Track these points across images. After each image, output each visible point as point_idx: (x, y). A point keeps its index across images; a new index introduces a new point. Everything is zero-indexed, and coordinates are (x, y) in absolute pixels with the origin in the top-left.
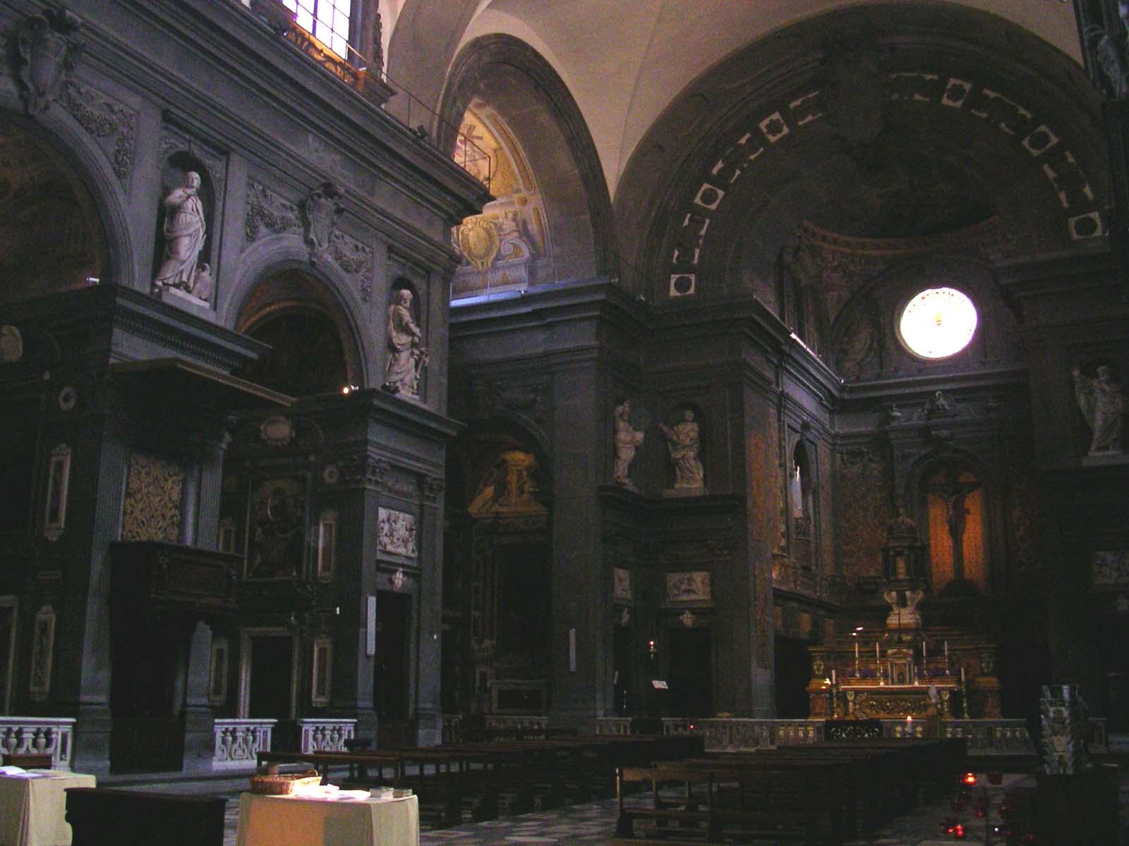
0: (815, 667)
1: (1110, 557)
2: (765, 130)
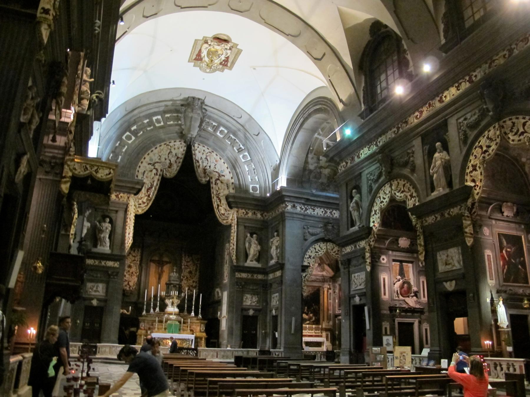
0: (140, 325)
1: (249, 296)
2: (155, 121)
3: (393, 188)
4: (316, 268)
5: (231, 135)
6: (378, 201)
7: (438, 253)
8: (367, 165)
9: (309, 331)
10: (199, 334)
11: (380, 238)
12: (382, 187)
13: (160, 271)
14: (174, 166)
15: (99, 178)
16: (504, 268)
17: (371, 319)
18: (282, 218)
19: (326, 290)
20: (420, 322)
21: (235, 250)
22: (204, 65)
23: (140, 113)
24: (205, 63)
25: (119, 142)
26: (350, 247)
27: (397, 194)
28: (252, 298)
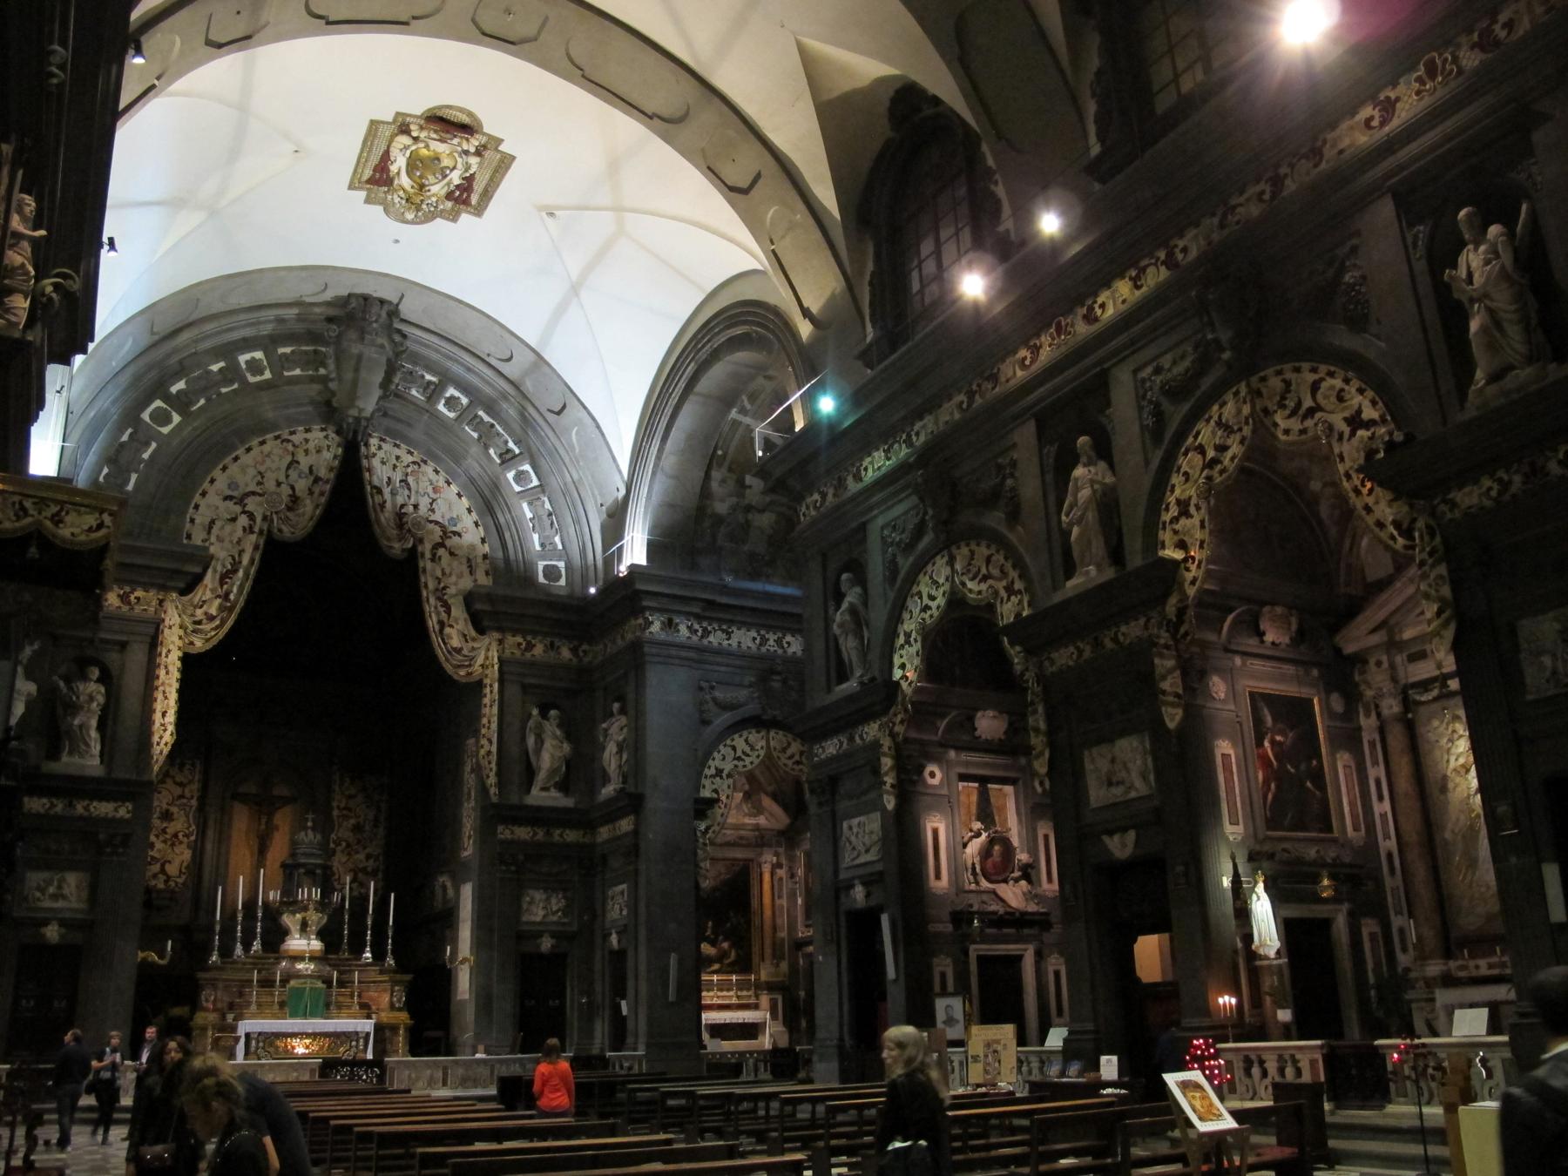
0: (203, 998)
1: (539, 895)
2: (244, 366)
3: (958, 567)
4: (739, 807)
5: (481, 413)
6: (914, 606)
7: (1086, 753)
8: (884, 501)
9: (719, 994)
10: (386, 1017)
11: (922, 712)
12: (927, 563)
13: (263, 827)
14: (305, 506)
15: (64, 540)
16: (1269, 789)
17: (901, 948)
18: (636, 656)
19: (766, 869)
20: (1039, 956)
21: (494, 758)
22: (397, 200)
23: (196, 341)
24: (401, 193)
25: (130, 431)
26: (835, 741)
27: (970, 585)
28: (548, 899)
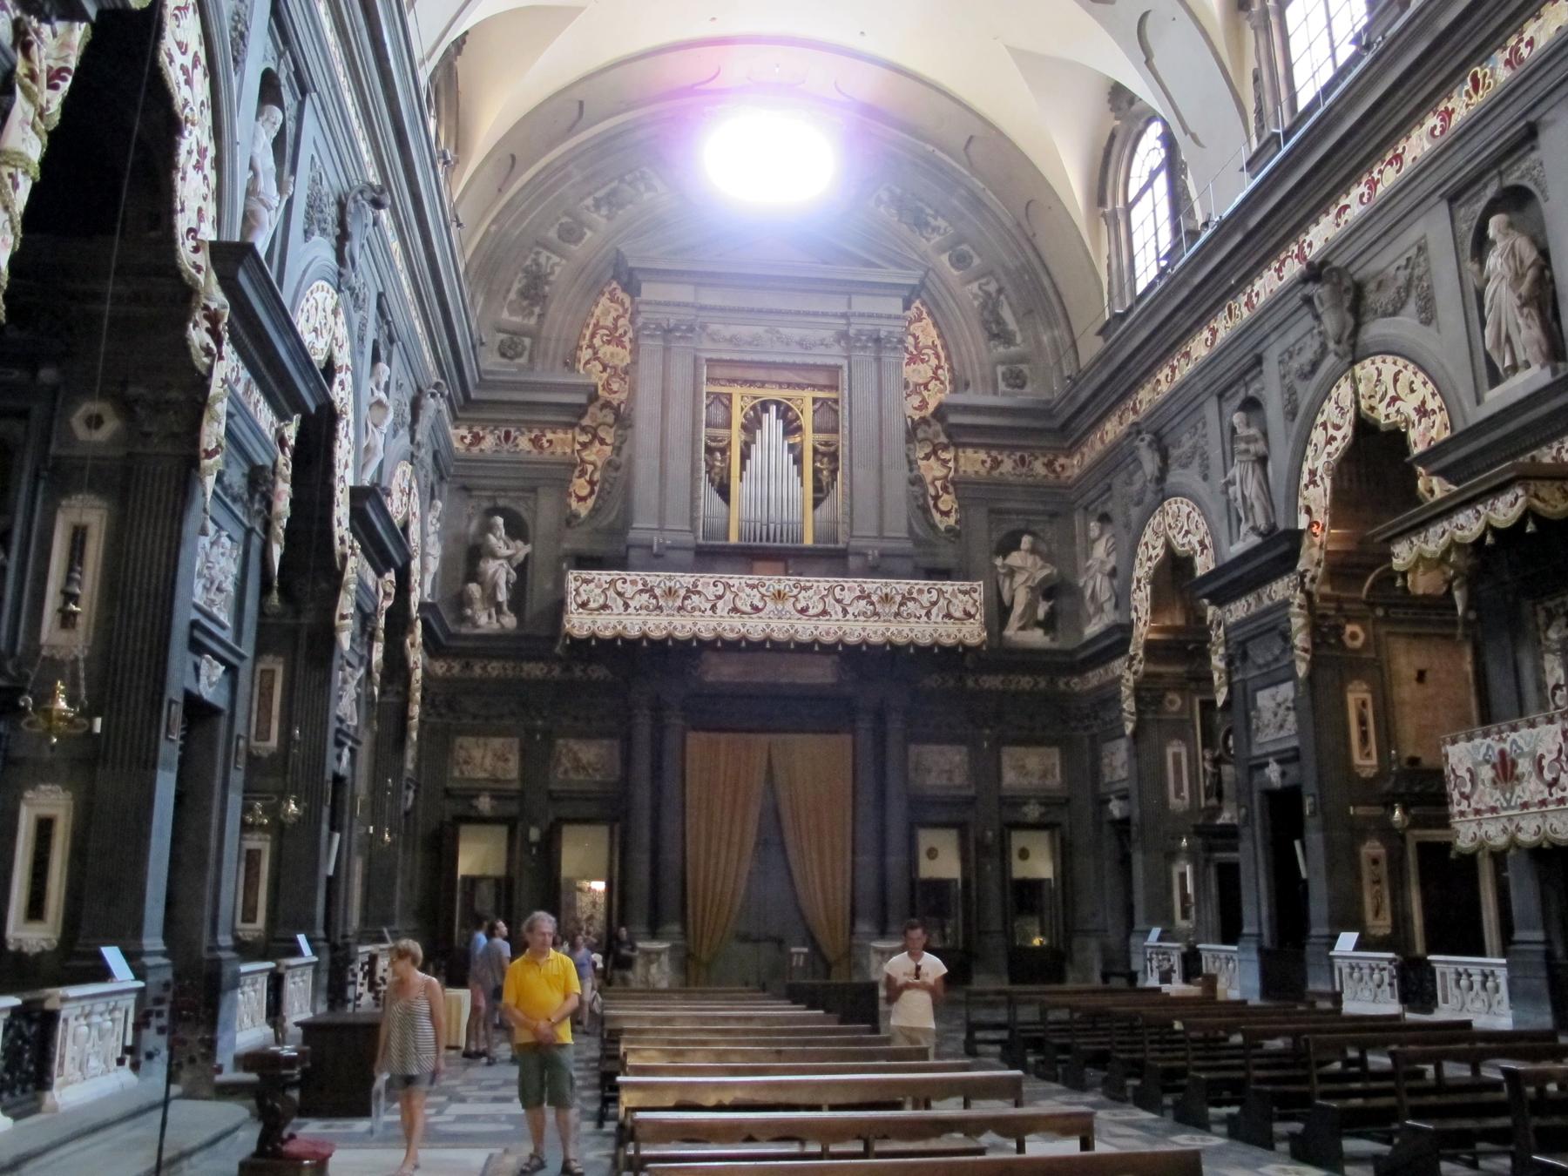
26: (1243, 602)
